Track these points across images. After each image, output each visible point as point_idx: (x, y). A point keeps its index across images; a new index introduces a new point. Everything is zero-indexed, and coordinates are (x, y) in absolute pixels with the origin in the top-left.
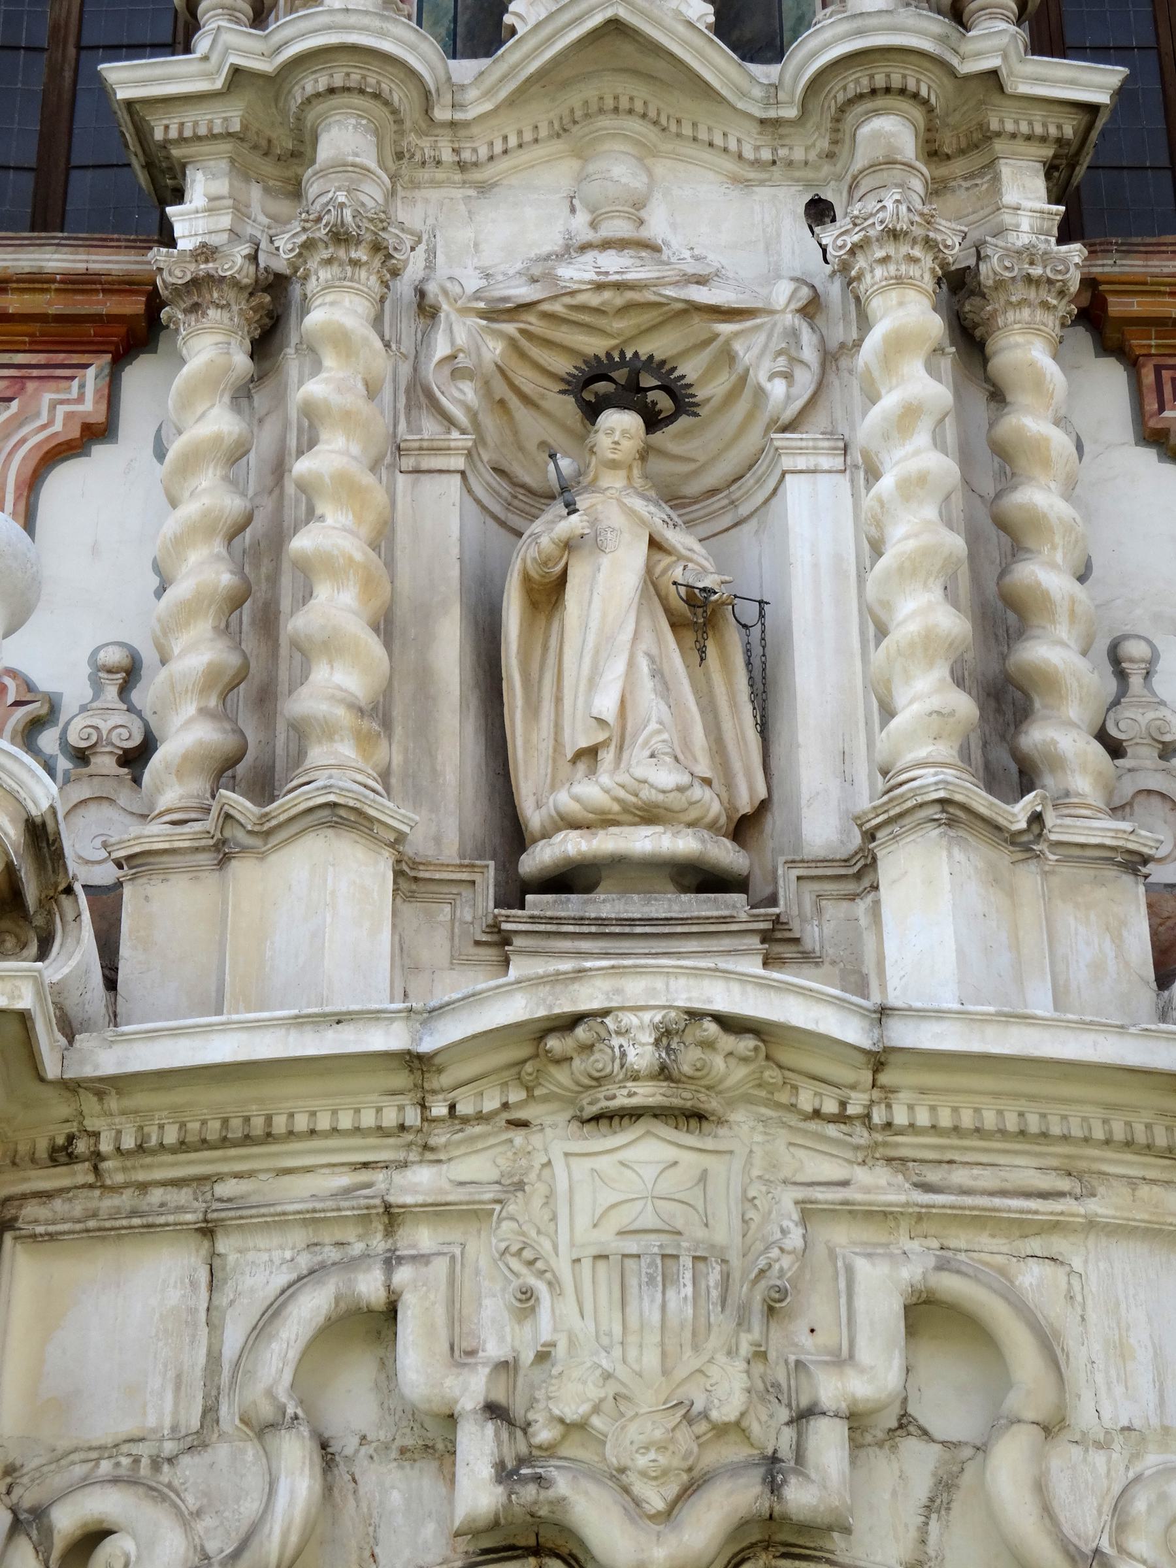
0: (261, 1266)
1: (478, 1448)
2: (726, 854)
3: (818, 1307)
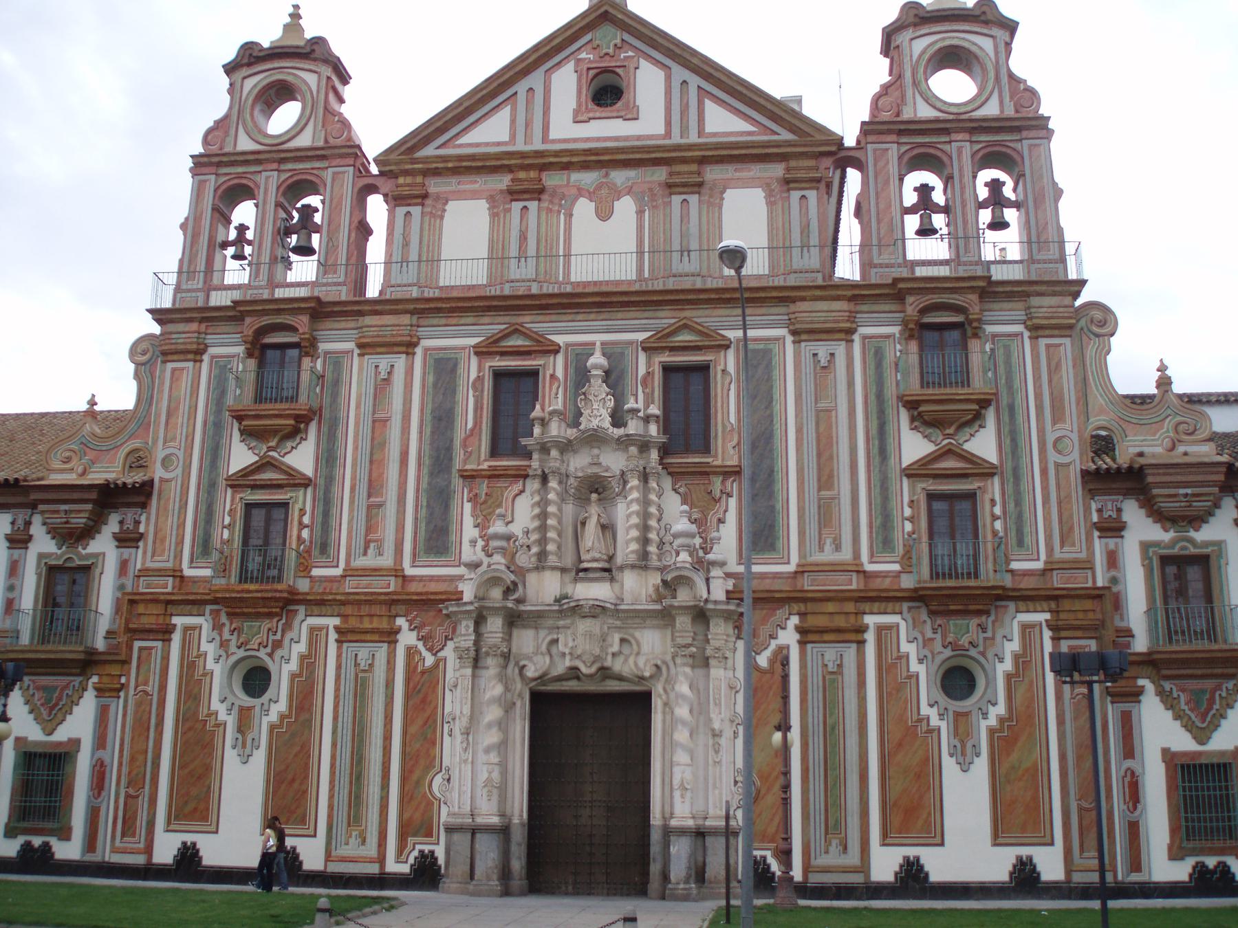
0: (542, 633)
1: (568, 658)
2: (606, 565)
3: (609, 639)
